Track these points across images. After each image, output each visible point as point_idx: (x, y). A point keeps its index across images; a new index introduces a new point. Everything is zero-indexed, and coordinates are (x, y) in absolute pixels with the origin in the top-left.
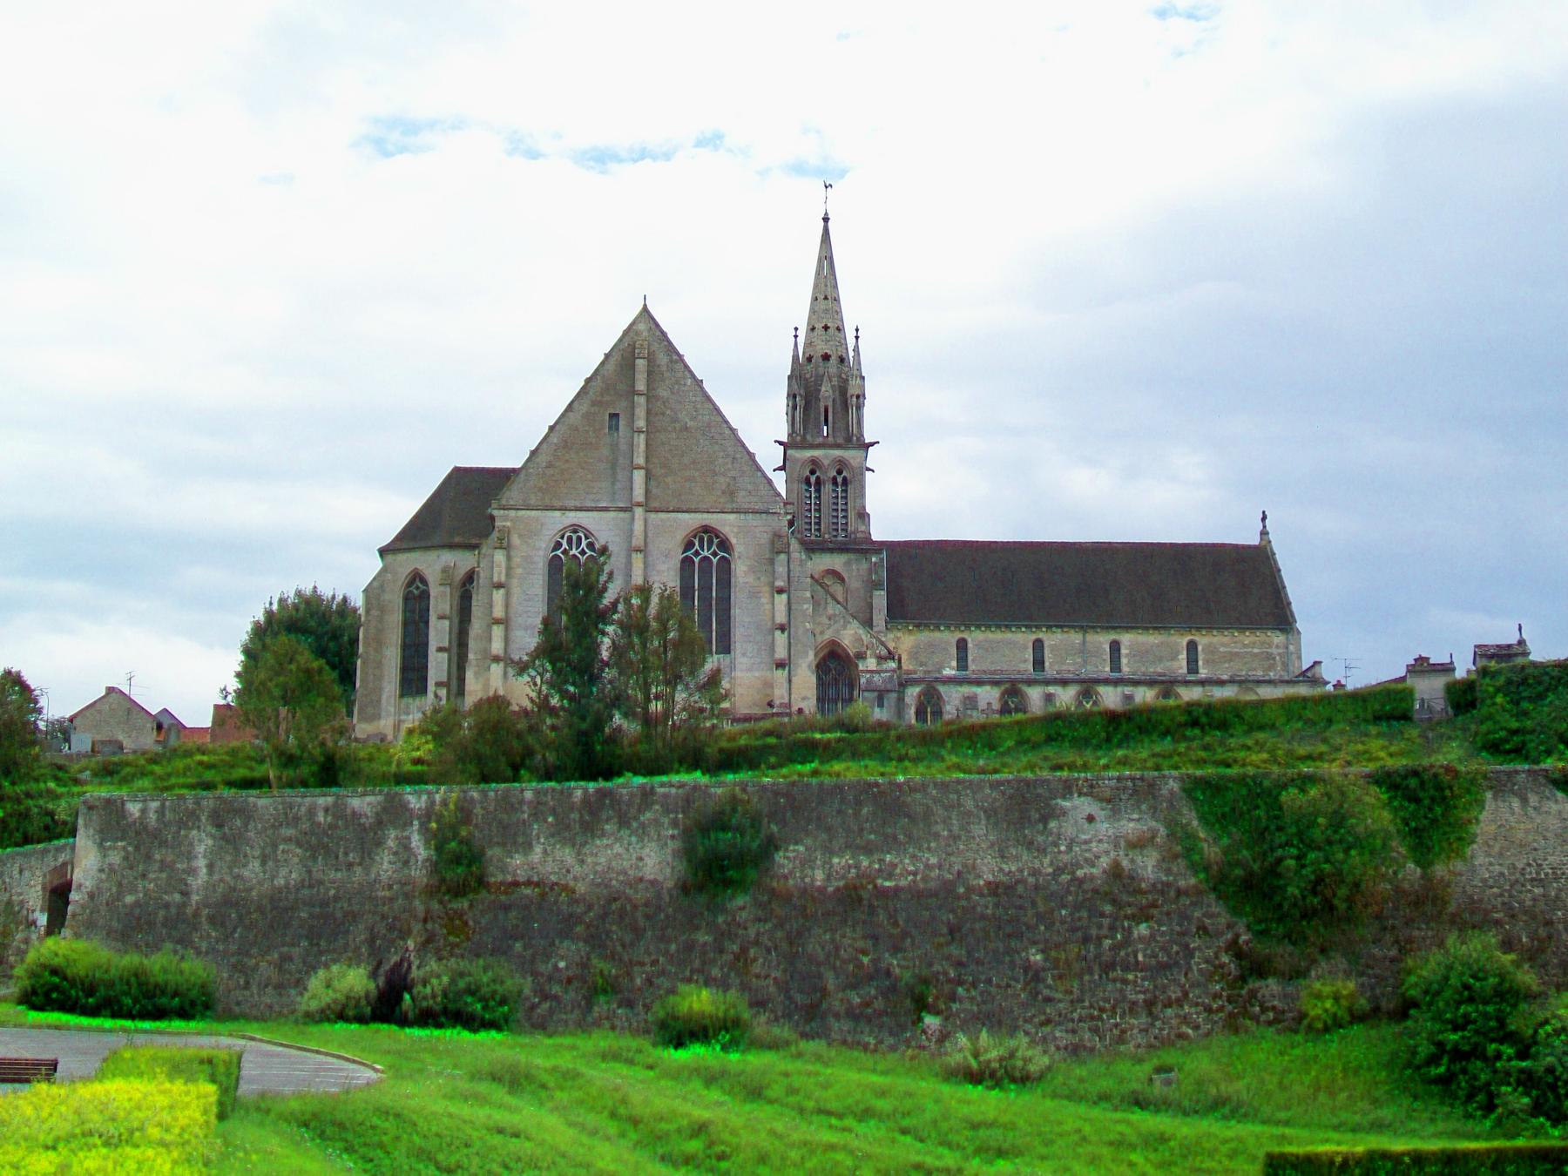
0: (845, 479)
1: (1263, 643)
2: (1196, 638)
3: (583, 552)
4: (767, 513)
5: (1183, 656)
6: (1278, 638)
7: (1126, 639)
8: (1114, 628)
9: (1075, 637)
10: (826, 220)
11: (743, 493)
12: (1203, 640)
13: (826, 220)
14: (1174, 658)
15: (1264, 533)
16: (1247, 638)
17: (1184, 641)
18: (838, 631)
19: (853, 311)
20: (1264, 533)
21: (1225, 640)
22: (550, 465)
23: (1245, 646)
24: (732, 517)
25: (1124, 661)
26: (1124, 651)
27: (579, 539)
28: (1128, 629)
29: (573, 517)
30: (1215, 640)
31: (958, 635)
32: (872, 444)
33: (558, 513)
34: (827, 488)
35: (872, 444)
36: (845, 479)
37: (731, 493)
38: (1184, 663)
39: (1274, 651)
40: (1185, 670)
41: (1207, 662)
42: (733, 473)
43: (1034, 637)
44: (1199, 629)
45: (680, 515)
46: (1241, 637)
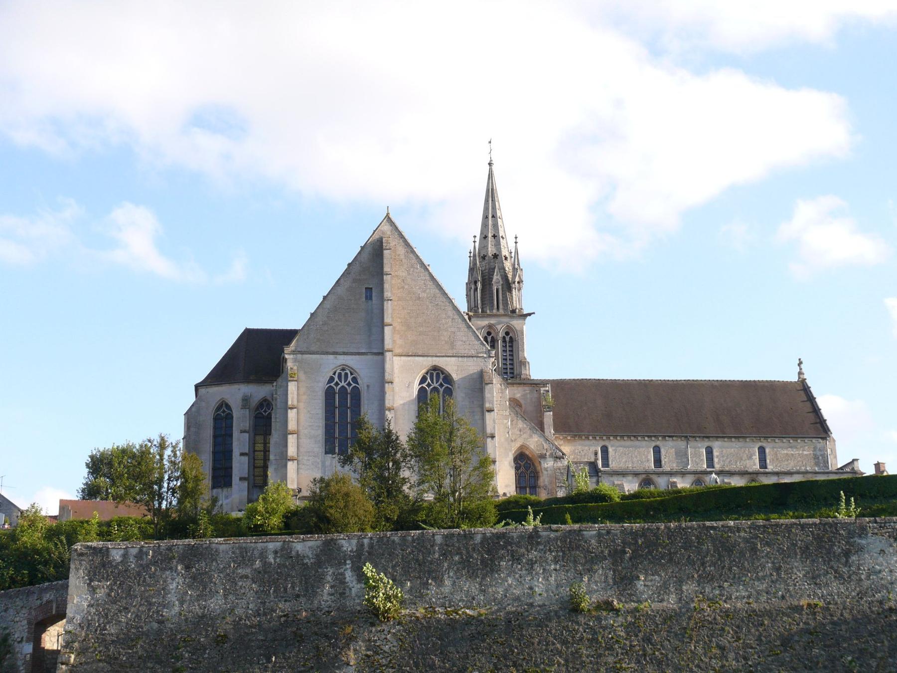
0: (511, 338)
2: (764, 445)
3: (349, 384)
8: (708, 437)
14: (750, 457)
19: (511, 226)
22: (325, 324)
25: (716, 460)
27: (346, 374)
29: (342, 360)
32: (530, 314)
33: (332, 356)
35: (530, 314)
36: (511, 338)
37: (452, 345)
42: (453, 329)
43: (654, 444)
45: (417, 358)
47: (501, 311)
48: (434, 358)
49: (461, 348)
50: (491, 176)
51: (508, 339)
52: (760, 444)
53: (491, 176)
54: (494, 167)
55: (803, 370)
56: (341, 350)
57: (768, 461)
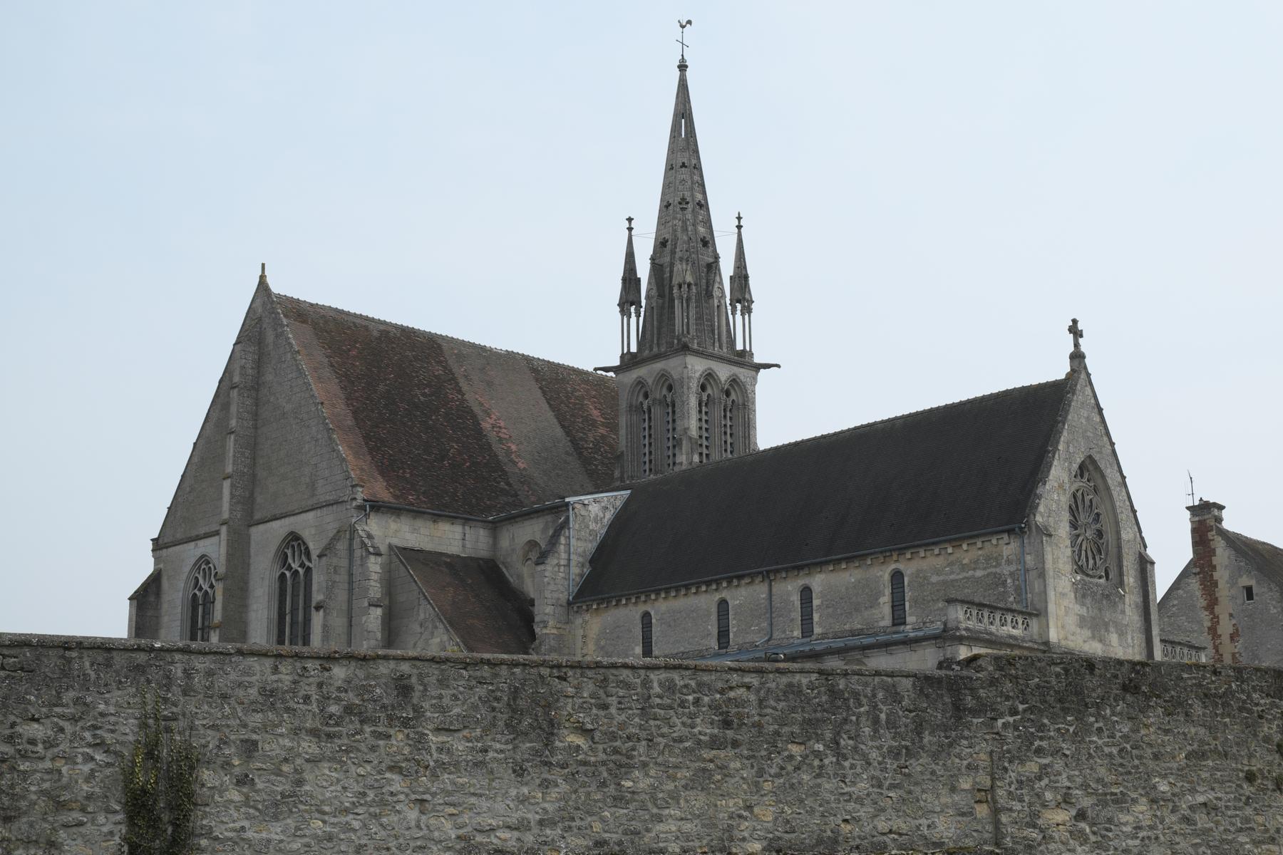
1: (988, 558)
2: (901, 566)
4: (337, 503)
5: (886, 599)
6: (1008, 547)
7: (818, 581)
8: (799, 568)
9: (759, 591)
10: (683, 67)
11: (321, 482)
12: (909, 567)
13: (683, 67)
14: (874, 603)
15: (1077, 357)
16: (968, 553)
17: (883, 574)
18: (427, 641)
20: (1077, 357)
21: (939, 562)
23: (964, 568)
24: (311, 515)
25: (816, 617)
26: (816, 602)
28: (820, 565)
30: (924, 565)
31: (642, 608)
34: (657, 411)
37: (312, 486)
38: (887, 610)
39: (1006, 570)
40: (887, 622)
41: (915, 601)
43: (717, 597)
44: (901, 551)
46: (959, 554)
47: (655, 350)
48: (292, 519)
49: (324, 494)
50: (683, 87)
51: (669, 400)
52: (893, 566)
53: (683, 87)
54: (689, 73)
55: (1084, 348)
56: (202, 531)
57: (907, 604)
